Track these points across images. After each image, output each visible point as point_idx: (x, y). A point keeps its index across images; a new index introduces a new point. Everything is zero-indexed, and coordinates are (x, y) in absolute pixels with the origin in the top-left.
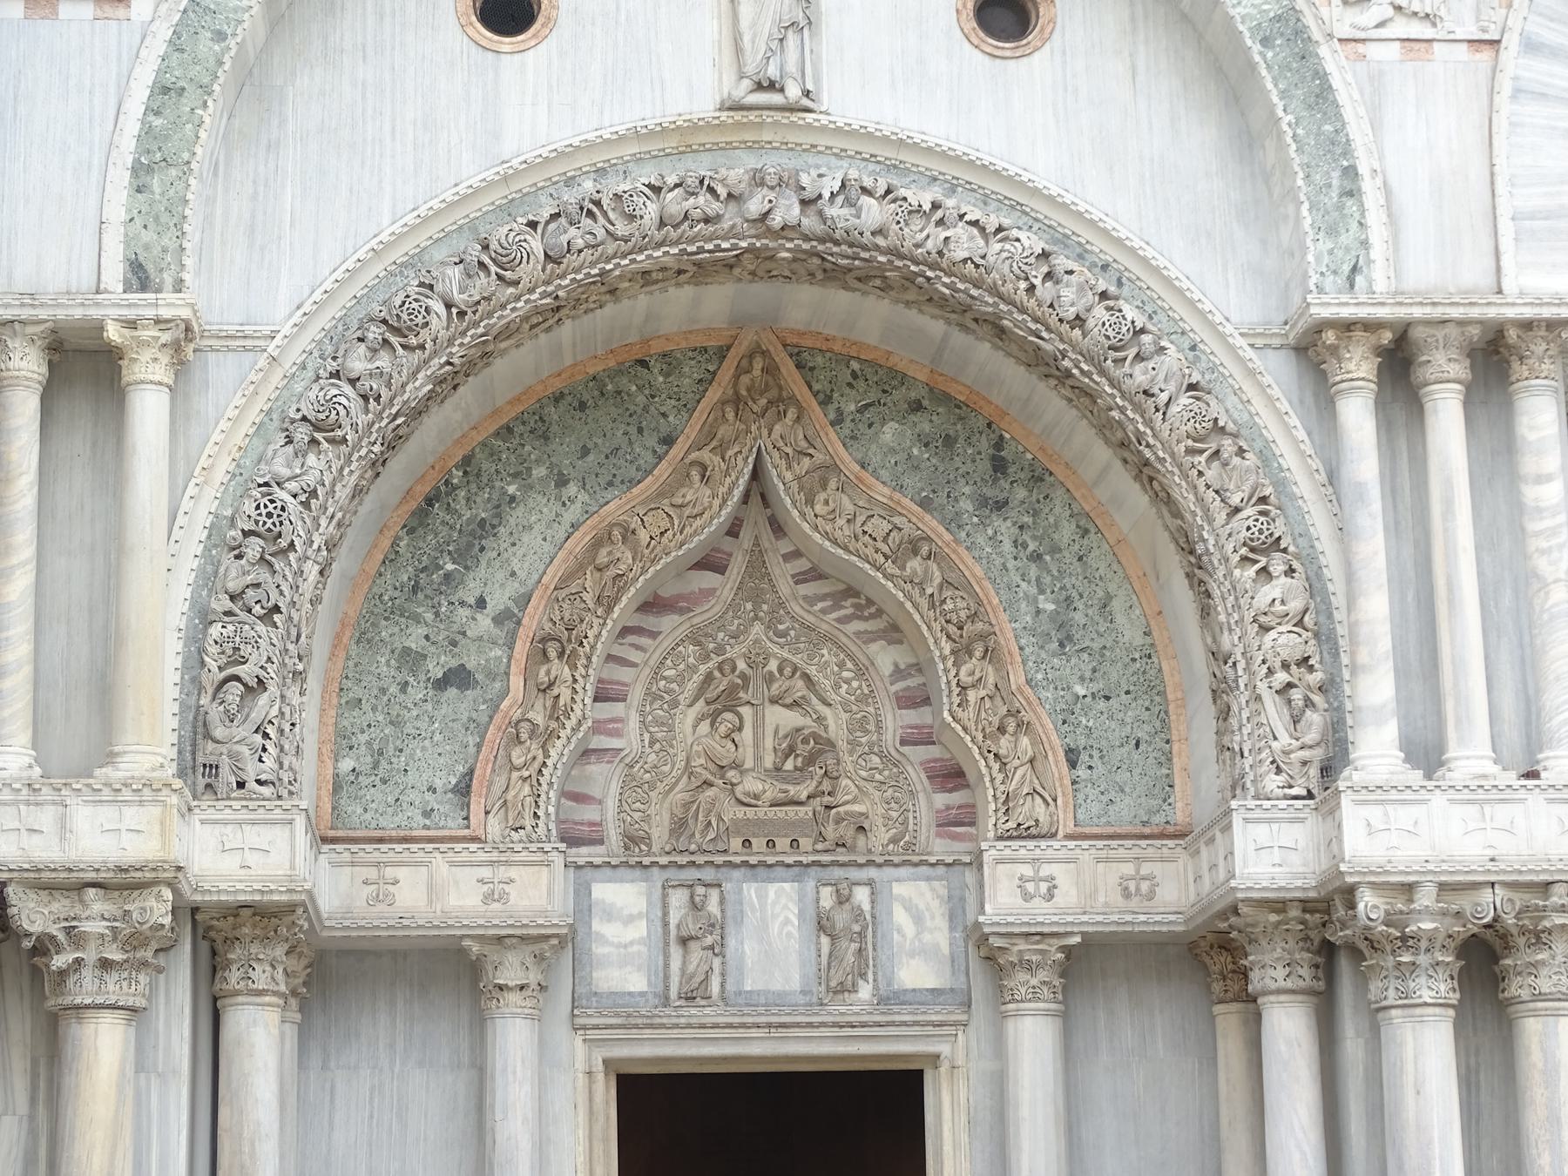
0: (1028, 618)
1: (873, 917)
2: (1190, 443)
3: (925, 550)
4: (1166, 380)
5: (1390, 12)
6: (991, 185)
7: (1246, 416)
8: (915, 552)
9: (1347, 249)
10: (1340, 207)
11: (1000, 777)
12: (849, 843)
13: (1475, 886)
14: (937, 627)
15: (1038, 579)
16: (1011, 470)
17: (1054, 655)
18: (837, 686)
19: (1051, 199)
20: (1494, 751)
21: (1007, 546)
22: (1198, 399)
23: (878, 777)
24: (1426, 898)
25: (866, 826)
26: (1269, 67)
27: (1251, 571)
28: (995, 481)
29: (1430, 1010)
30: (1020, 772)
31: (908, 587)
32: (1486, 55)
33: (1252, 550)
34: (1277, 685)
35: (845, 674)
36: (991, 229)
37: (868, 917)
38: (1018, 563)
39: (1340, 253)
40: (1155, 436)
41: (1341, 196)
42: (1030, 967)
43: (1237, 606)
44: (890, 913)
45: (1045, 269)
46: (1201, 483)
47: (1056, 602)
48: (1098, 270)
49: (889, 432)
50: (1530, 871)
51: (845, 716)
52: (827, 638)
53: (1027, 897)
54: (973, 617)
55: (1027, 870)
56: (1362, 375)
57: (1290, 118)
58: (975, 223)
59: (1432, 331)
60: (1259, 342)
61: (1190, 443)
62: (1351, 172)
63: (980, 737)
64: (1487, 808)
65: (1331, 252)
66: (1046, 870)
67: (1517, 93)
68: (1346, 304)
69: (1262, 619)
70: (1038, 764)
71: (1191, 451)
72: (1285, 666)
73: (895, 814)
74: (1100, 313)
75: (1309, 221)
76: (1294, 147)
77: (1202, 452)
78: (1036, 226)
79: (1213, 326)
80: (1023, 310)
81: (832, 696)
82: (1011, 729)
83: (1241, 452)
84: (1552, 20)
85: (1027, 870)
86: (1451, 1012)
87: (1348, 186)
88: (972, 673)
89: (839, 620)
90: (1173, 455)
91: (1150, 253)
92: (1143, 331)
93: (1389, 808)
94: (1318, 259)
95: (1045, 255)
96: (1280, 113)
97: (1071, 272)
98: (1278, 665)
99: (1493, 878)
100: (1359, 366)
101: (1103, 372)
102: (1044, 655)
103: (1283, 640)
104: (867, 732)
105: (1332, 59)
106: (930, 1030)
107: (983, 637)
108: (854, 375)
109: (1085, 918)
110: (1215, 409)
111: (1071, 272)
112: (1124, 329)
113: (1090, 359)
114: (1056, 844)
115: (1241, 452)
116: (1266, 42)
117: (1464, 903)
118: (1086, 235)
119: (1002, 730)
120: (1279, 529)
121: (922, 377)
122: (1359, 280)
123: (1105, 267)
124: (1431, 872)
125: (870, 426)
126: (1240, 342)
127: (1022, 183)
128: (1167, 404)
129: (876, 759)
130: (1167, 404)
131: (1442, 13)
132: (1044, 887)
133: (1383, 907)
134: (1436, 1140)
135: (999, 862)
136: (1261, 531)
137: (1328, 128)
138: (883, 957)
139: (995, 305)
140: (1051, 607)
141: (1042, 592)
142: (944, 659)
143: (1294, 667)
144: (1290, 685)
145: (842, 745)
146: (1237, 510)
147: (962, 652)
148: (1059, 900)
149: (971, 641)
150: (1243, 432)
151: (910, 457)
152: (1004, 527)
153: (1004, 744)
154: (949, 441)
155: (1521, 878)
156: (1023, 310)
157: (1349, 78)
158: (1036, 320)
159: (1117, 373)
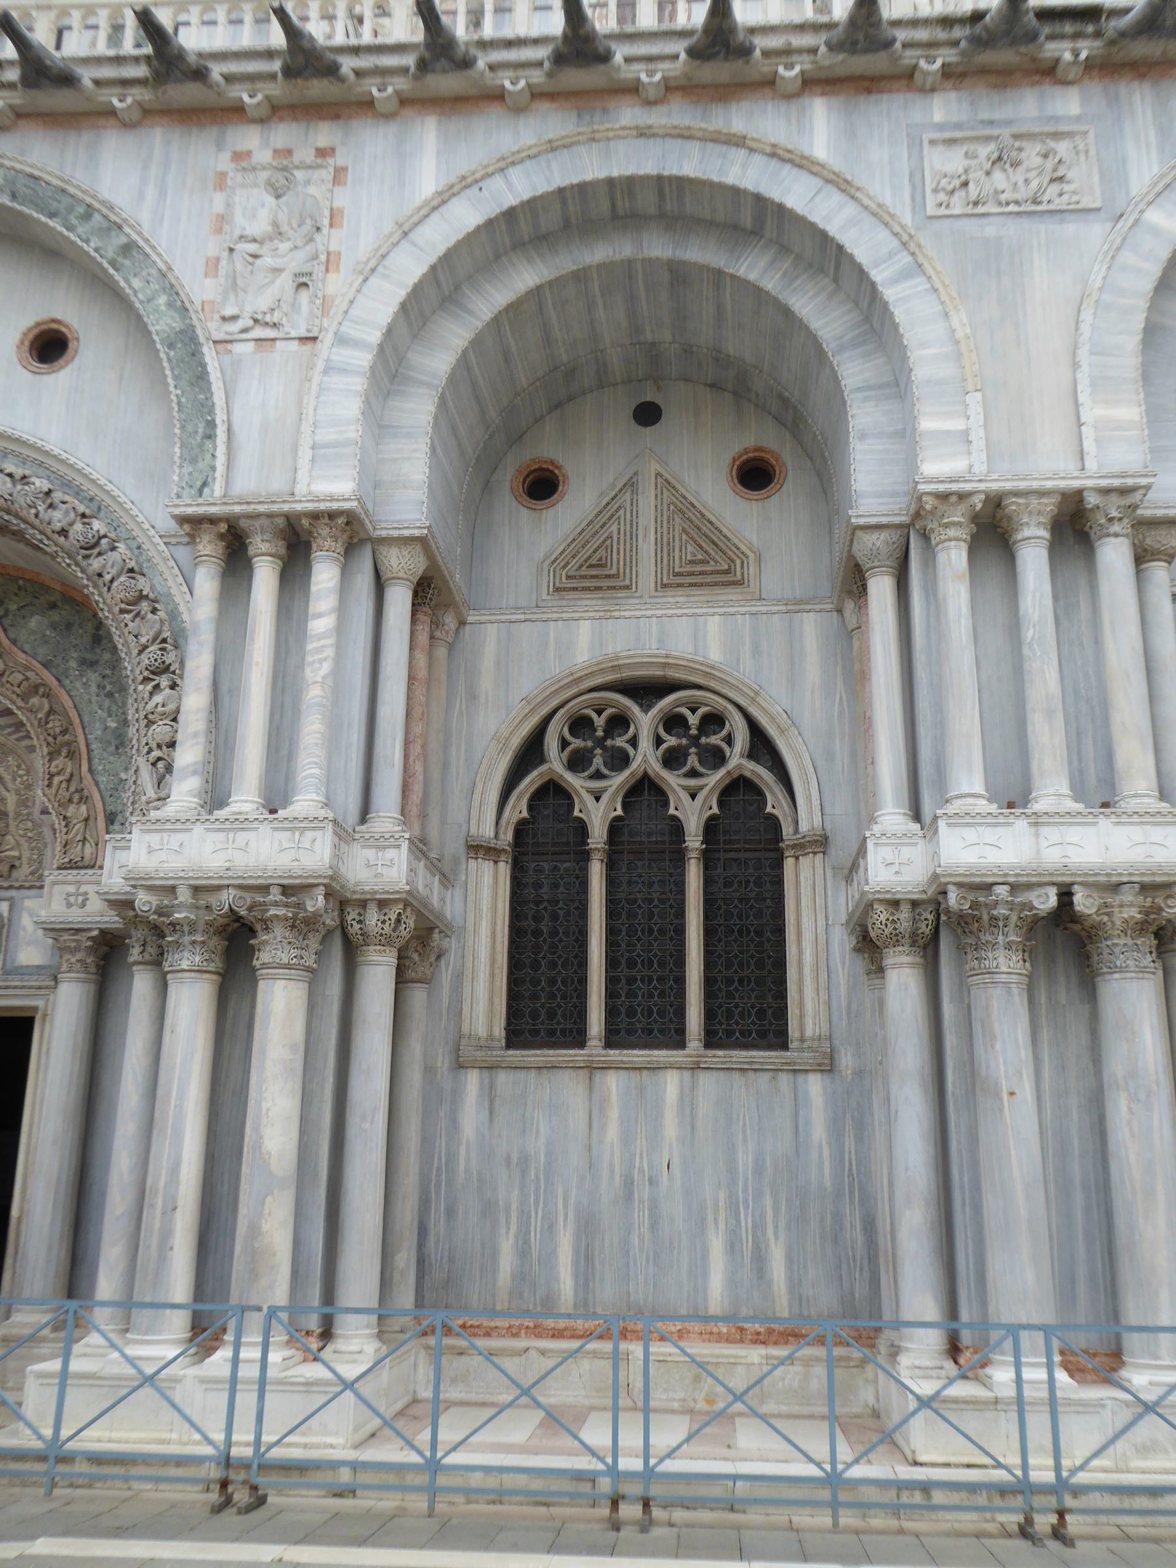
0: (99, 732)
1: (9, 920)
2: (123, 606)
3: (41, 690)
4: (112, 567)
5: (251, 323)
6: (26, 452)
7: (165, 590)
8: (36, 693)
9: (201, 472)
10: (201, 445)
11: (65, 830)
12: (5, 874)
13: (219, 888)
14: (42, 737)
15: (109, 709)
16: (104, 642)
17: (112, 754)
18: (14, 779)
19: (55, 457)
20: (402, 814)
21: (94, 689)
22: (133, 578)
23: (29, 834)
24: (184, 896)
25: (17, 863)
26: (169, 360)
27: (149, 687)
28: (93, 648)
29: (187, 975)
30: (76, 828)
31: (29, 714)
32: (308, 347)
33: (153, 673)
34: (151, 759)
35: (21, 772)
36: (18, 477)
37: (6, 921)
38: (99, 699)
39: (196, 474)
40: (104, 603)
41: (203, 438)
42: (73, 951)
43: (137, 710)
44: (20, 918)
45: (49, 501)
46: (126, 631)
47: (118, 722)
48: (86, 502)
49: (34, 622)
50: (250, 877)
51: (15, 797)
52: (12, 751)
53: (69, 905)
54: (65, 732)
55: (71, 889)
56: (206, 553)
57: (179, 392)
58: (10, 475)
59: (252, 522)
60: (173, 540)
61: (123, 606)
62: (212, 424)
63: (56, 805)
64: (231, 835)
65: (190, 474)
66: (83, 889)
67: (327, 370)
68: (190, 505)
69: (151, 717)
70: (91, 822)
71: (122, 611)
72: (159, 746)
73: (35, 857)
74: (78, 527)
75: (178, 454)
76: (176, 409)
77: (129, 612)
78: (53, 476)
79: (144, 531)
80: (33, 527)
81: (10, 785)
82: (75, 801)
83: (154, 611)
84: (358, 323)
85: (71, 889)
86: (215, 977)
87: (208, 432)
88: (57, 767)
89: (17, 740)
90: (113, 614)
91: (110, 487)
92: (105, 536)
93: (165, 835)
94: (181, 478)
95: (48, 493)
96: (172, 388)
97: (64, 503)
98: (154, 746)
99: (226, 882)
100: (209, 546)
101: (77, 564)
102: (105, 755)
103: (159, 730)
104: (27, 807)
105: (209, 354)
106: (33, 992)
107: (68, 744)
108: (20, 588)
109: (98, 919)
110: (143, 584)
111: (64, 503)
112: (90, 536)
113: (70, 557)
114: (90, 872)
115: (154, 611)
116: (171, 346)
117: (213, 900)
118: (79, 480)
119: (70, 801)
120: (170, 658)
121: (57, 587)
122: (206, 491)
123: (91, 500)
124: (181, 878)
125: (24, 618)
126: (157, 540)
127: (47, 452)
128: (112, 581)
129: (29, 824)
130: (112, 581)
131: (284, 321)
132: (80, 899)
133: (155, 903)
134: (178, 1065)
135: (55, 883)
136: (156, 660)
137: (202, 397)
138: (11, 945)
139: (18, 525)
140: (114, 725)
141: (110, 715)
142: (43, 757)
143: (164, 748)
144: (159, 759)
145: (11, 815)
146: (145, 647)
147: (52, 756)
148: (89, 907)
149: (62, 745)
150: (163, 599)
151: (44, 635)
152: (93, 677)
153: (71, 811)
154: (69, 626)
155: (245, 882)
156: (33, 527)
157: (217, 365)
158: (42, 533)
159: (84, 563)
